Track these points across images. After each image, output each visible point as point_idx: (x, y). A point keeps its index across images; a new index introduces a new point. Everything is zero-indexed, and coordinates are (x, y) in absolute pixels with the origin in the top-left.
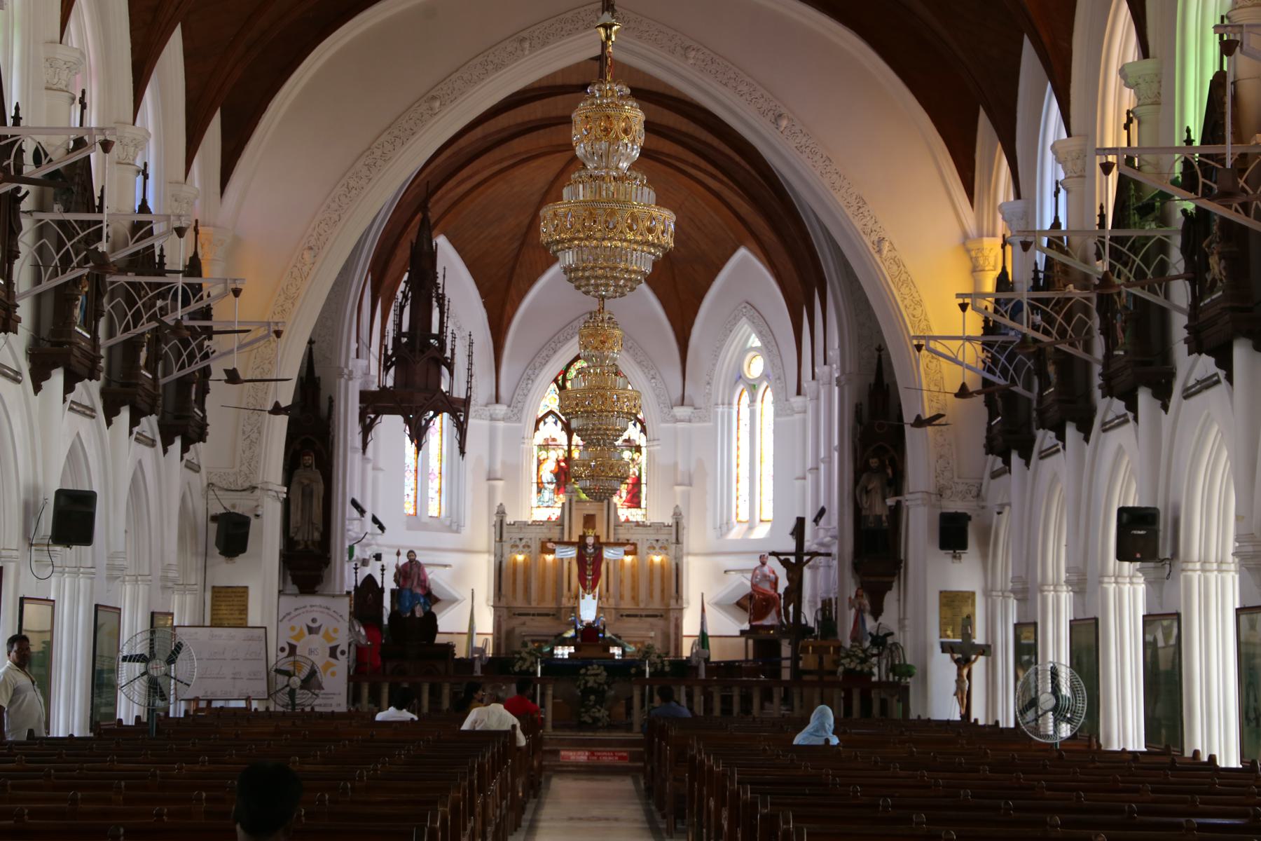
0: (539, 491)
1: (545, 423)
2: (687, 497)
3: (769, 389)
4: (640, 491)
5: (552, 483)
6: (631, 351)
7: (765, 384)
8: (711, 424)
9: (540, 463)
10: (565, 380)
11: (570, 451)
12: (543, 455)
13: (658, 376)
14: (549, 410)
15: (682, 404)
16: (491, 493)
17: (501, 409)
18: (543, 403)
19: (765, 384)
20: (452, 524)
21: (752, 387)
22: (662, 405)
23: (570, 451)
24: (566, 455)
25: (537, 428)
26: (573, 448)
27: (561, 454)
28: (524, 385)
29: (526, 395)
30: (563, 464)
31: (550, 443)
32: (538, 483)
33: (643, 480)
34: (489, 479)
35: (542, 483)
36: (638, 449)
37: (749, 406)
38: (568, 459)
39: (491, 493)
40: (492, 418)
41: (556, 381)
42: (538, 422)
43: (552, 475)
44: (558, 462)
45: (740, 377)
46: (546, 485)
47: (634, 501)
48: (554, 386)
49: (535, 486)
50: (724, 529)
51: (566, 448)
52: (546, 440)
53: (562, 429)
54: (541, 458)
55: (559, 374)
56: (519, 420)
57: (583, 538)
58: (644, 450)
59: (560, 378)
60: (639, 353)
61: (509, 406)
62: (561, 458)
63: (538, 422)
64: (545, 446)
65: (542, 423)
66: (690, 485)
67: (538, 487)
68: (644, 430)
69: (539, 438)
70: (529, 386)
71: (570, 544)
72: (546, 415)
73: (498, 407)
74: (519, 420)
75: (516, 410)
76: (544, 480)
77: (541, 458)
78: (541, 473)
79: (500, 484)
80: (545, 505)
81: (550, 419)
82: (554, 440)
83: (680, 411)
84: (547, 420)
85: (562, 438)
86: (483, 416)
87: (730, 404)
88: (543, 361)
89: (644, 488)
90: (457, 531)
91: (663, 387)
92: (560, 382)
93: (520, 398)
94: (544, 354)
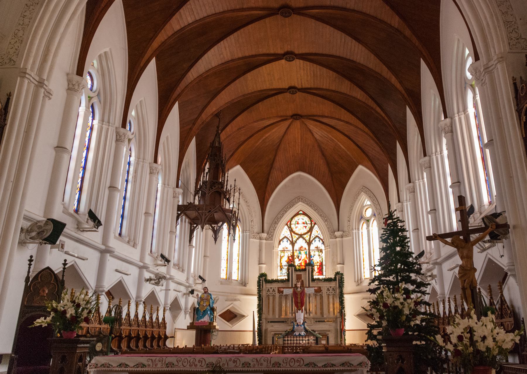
0: (281, 269)
1: (283, 242)
2: (343, 268)
3: (375, 221)
4: (323, 268)
5: (286, 266)
6: (317, 211)
7: (373, 219)
8: (350, 238)
9: (281, 258)
10: (290, 224)
11: (293, 253)
12: (282, 254)
13: (328, 220)
14: (284, 236)
15: (339, 231)
16: (260, 269)
17: (264, 235)
18: (282, 234)
19: (373, 219)
20: (243, 283)
21: (368, 221)
22: (330, 232)
23: (293, 253)
24: (292, 254)
25: (279, 244)
26: (294, 251)
27: (290, 254)
28: (274, 226)
29: (274, 230)
30: (290, 258)
31: (285, 249)
32: (280, 266)
33: (324, 264)
34: (259, 264)
35: (282, 266)
36: (321, 251)
37: (367, 228)
38: (293, 256)
39: (260, 269)
40: (261, 239)
41: (287, 224)
42: (280, 242)
43: (286, 263)
44: (289, 257)
45: (361, 217)
46: (284, 267)
47: (321, 272)
48: (286, 227)
49: (279, 267)
50: (359, 282)
51: (292, 251)
52: (284, 248)
53: (290, 244)
54: (282, 256)
55: (288, 222)
56: (272, 240)
57: (296, 285)
58: (324, 251)
59: (289, 223)
60: (320, 212)
61: (268, 234)
62: (290, 255)
63: (280, 242)
64: (283, 251)
65: (282, 241)
66: (343, 264)
67: (280, 268)
68: (323, 243)
69: (281, 248)
70: (276, 226)
71: (292, 287)
72: (283, 238)
73: (263, 234)
74: (272, 240)
75: (270, 236)
76: (283, 265)
77: (282, 256)
78: (281, 262)
79: (264, 266)
80: (283, 275)
81: (285, 240)
82: (287, 248)
83: (337, 234)
84: (284, 240)
85: (290, 247)
86: (257, 238)
87: (358, 229)
88: (281, 216)
89: (324, 267)
90: (245, 286)
91: (330, 224)
92: (289, 225)
93: (272, 231)
94: (281, 213)
